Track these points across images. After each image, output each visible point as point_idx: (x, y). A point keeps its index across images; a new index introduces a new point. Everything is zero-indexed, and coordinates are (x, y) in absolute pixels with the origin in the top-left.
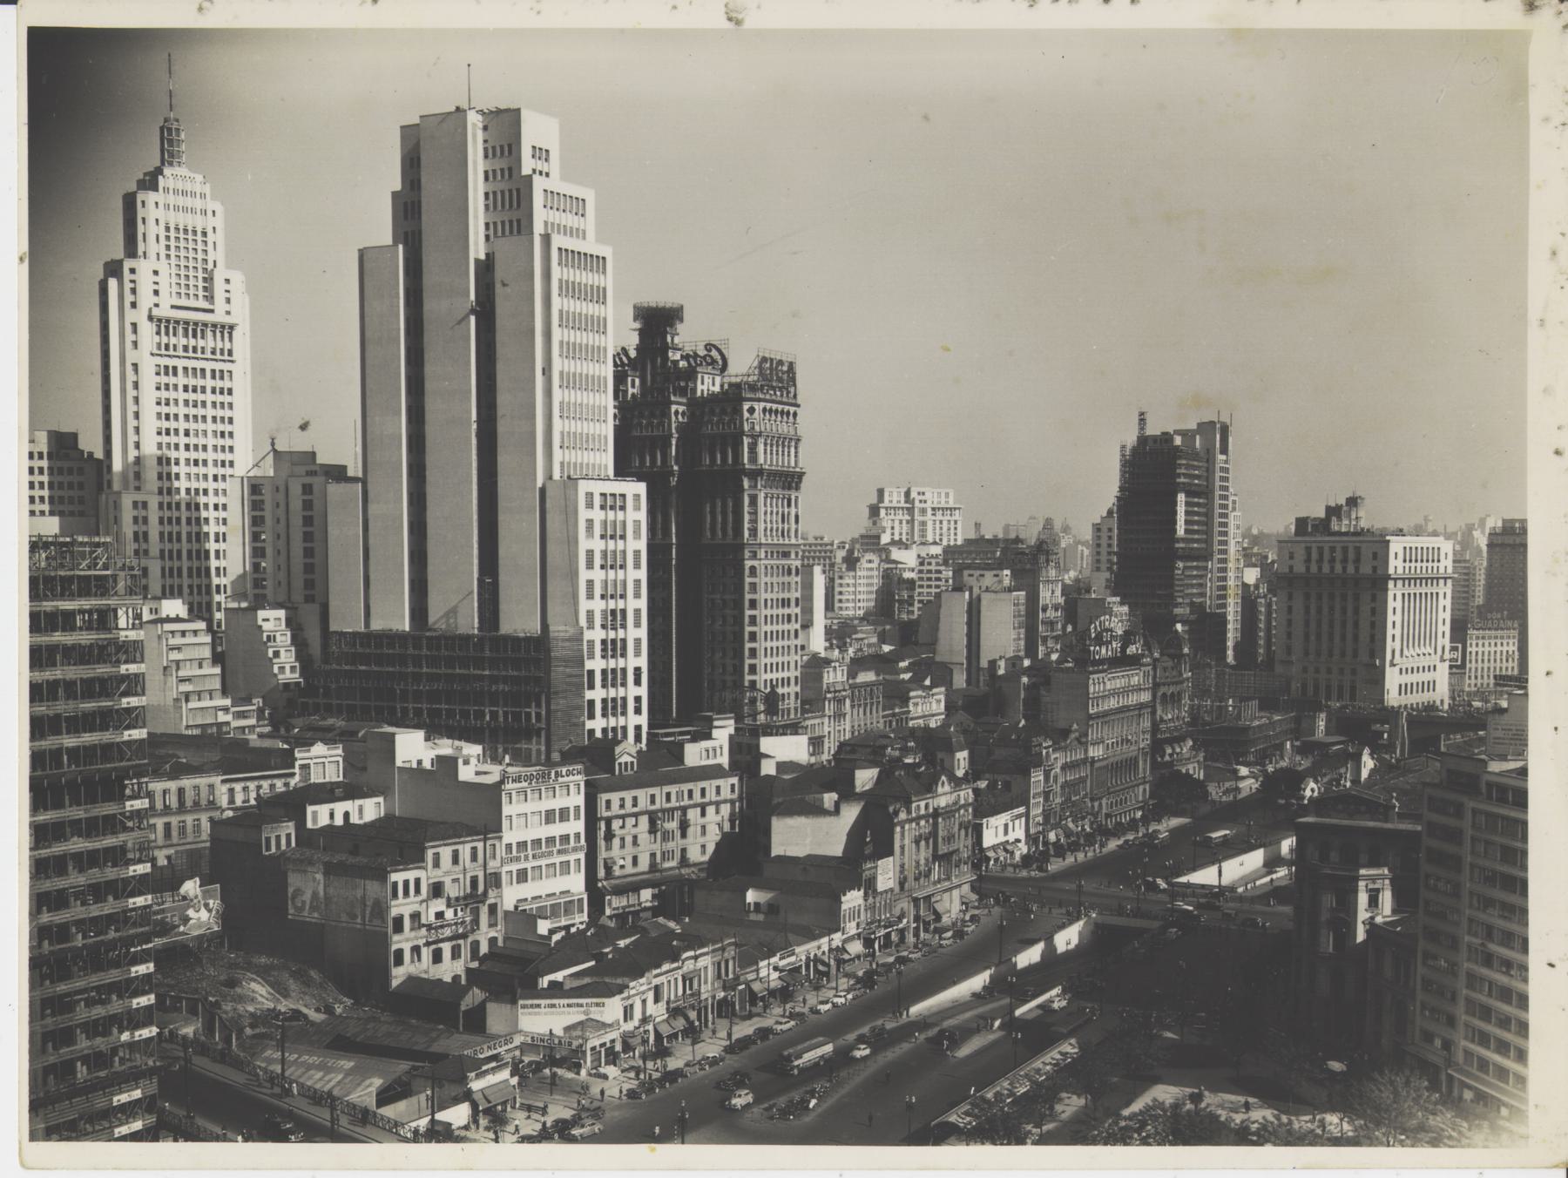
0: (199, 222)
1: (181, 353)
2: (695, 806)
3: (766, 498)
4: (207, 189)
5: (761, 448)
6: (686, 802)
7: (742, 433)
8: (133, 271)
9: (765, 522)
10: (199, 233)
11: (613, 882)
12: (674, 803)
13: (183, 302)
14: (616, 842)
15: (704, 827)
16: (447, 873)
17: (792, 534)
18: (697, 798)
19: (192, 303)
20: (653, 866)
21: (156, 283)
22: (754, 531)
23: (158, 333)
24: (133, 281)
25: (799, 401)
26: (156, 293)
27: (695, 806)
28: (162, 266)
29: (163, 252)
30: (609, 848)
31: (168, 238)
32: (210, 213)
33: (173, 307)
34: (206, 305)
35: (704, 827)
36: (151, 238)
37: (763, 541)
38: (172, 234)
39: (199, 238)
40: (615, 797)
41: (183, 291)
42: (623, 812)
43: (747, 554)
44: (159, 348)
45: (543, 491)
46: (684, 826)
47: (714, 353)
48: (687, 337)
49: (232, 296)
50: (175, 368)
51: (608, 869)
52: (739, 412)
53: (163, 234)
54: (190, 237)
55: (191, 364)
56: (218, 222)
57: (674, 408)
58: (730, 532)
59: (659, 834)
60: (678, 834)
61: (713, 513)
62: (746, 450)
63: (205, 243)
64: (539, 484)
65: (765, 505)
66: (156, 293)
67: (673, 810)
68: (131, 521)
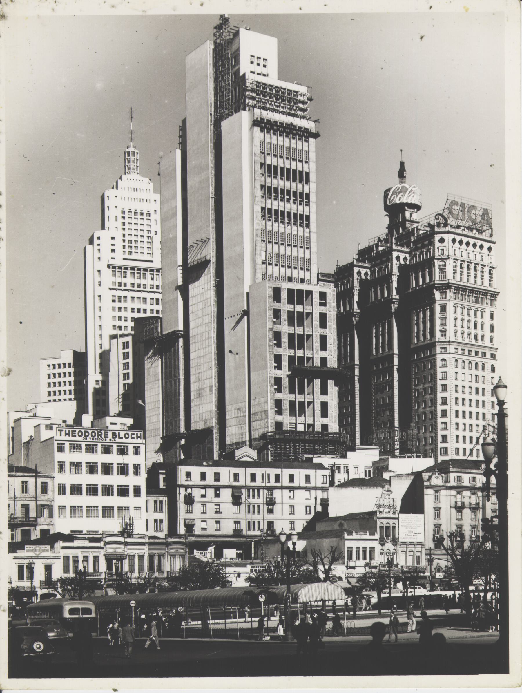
0: (145, 207)
2: (282, 488)
4: (151, 186)
5: (449, 269)
6: (273, 483)
7: (433, 258)
8: (99, 238)
10: (145, 214)
11: (193, 539)
12: (258, 482)
14: (197, 508)
15: (292, 507)
17: (487, 339)
18: (285, 481)
20: (237, 533)
22: (444, 332)
24: (99, 245)
26: (113, 251)
27: (282, 488)
29: (120, 227)
30: (189, 512)
33: (124, 259)
34: (149, 258)
35: (292, 507)
36: (112, 219)
37: (453, 339)
39: (145, 217)
40: (196, 471)
42: (203, 483)
43: (438, 350)
45: (248, 294)
46: (271, 502)
51: (189, 528)
52: (432, 243)
53: (120, 215)
54: (139, 216)
56: (158, 206)
57: (395, 254)
58: (428, 336)
59: (243, 506)
60: (264, 509)
61: (418, 324)
64: (247, 290)
65: (455, 312)
66: (113, 251)
67: (259, 488)
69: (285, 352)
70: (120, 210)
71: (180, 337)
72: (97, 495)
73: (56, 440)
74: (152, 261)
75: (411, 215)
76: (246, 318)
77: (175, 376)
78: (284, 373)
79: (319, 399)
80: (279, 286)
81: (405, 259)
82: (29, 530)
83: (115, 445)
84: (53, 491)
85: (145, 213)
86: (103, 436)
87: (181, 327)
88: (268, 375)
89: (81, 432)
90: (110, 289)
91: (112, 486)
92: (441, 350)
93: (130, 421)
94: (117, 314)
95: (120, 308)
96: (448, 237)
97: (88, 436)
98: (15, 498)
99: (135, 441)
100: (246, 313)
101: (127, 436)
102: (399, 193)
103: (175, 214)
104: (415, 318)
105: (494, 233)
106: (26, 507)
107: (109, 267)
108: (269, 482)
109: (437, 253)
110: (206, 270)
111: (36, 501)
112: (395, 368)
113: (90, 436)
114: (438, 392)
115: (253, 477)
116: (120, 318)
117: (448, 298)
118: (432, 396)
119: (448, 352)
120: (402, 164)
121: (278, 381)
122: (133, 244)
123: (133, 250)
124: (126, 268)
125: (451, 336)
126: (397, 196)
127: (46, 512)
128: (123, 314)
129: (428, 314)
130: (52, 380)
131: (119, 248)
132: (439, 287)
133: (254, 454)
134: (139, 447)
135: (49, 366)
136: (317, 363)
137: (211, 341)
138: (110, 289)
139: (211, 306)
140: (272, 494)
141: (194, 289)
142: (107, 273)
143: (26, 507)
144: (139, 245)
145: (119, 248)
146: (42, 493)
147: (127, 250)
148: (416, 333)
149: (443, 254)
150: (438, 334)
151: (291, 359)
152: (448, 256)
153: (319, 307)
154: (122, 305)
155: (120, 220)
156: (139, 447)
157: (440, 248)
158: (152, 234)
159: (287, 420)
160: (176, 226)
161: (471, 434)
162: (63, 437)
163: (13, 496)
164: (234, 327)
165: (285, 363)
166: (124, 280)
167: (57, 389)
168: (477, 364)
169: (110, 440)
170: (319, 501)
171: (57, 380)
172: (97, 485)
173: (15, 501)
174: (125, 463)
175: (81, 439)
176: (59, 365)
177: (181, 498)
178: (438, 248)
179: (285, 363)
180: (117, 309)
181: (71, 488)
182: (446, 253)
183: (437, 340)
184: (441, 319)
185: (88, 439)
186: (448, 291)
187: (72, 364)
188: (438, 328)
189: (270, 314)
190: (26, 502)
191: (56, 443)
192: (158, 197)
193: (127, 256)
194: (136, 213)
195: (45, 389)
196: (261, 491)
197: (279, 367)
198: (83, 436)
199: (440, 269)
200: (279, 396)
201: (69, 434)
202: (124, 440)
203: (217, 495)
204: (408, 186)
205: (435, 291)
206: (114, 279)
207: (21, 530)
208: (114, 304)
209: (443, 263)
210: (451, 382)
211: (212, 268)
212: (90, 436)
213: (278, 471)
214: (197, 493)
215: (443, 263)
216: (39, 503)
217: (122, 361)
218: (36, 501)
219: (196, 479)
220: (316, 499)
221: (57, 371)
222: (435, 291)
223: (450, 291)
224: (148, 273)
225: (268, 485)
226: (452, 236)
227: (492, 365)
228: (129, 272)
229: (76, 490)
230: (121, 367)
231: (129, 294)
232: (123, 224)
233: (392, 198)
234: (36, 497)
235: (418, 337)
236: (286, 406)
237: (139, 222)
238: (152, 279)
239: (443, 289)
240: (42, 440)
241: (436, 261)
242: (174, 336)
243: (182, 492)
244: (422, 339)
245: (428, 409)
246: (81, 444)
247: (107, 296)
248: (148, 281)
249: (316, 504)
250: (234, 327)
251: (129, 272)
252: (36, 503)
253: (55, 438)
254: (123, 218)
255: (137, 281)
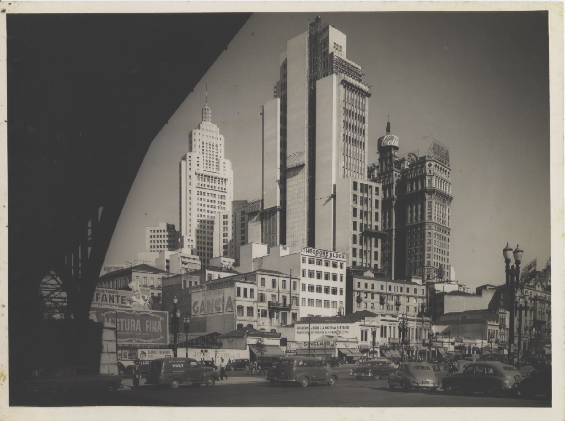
0: (215, 142)
2: (404, 296)
3: (436, 203)
6: (399, 292)
9: (435, 214)
10: (215, 146)
12: (392, 292)
13: (208, 169)
15: (408, 307)
16: (268, 291)
21: (198, 162)
22: (430, 217)
24: (190, 161)
26: (198, 165)
29: (201, 152)
35: (408, 307)
37: (434, 221)
39: (215, 147)
42: (366, 290)
43: (427, 227)
46: (398, 304)
53: (201, 145)
54: (211, 147)
55: (208, 191)
58: (419, 219)
59: (385, 305)
60: (395, 307)
61: (411, 213)
62: (427, 182)
64: (334, 182)
66: (198, 165)
69: (358, 220)
71: (278, 211)
72: (321, 292)
73: (302, 255)
74: (219, 173)
75: (394, 152)
76: (332, 199)
77: (273, 233)
78: (358, 232)
79: (374, 249)
80: (356, 181)
81: (399, 176)
82: (286, 313)
83: (331, 261)
84: (299, 288)
85: (215, 145)
86: (325, 254)
87: (278, 204)
88: (350, 233)
89: (314, 251)
90: (196, 187)
91: (329, 287)
92: (428, 227)
93: (233, 261)
94: (200, 202)
95: (201, 199)
96: (433, 164)
97: (318, 254)
98: (279, 291)
99: (341, 259)
100: (334, 196)
101: (337, 256)
102: (390, 139)
103: (277, 137)
104: (409, 209)
105: (450, 164)
106: (284, 298)
107: (196, 174)
108: (397, 291)
109: (427, 172)
110: (301, 171)
111: (290, 294)
112: (394, 237)
113: (319, 254)
114: (426, 251)
115: (390, 287)
116: (201, 205)
117: (433, 198)
118: (421, 253)
119: (432, 228)
120: (389, 124)
121: (355, 237)
122: (208, 163)
123: (208, 166)
124: (205, 176)
125: (433, 220)
126: (388, 141)
127: (295, 301)
128: (203, 202)
129: (420, 206)
130: (153, 239)
131: (201, 163)
132: (429, 191)
133: (372, 275)
134: (343, 263)
135: (151, 231)
136: (373, 228)
137: (304, 213)
138: (196, 187)
139: (304, 192)
140: (398, 299)
141: (291, 182)
142: (195, 177)
143: (284, 298)
144: (211, 163)
146: (293, 289)
147: (205, 166)
148: (415, 216)
150: (427, 218)
151: (361, 225)
152: (434, 174)
153: (375, 196)
154: (203, 197)
155: (201, 148)
156: (343, 263)
157: (429, 169)
158: (218, 158)
159: (358, 260)
160: (277, 144)
162: (305, 253)
163: (278, 290)
164: (324, 204)
165: (358, 227)
166: (204, 183)
167: (156, 244)
169: (329, 257)
170: (420, 304)
171: (156, 239)
172: (321, 286)
173: (279, 293)
174: (336, 273)
175: (314, 255)
176: (158, 231)
177: (355, 298)
178: (428, 169)
179: (358, 227)
180: (200, 199)
181: (308, 287)
182: (432, 172)
183: (426, 221)
184: (428, 210)
185: (318, 256)
186: (433, 194)
187: (166, 230)
188: (427, 215)
189: (351, 197)
190: (285, 294)
191: (301, 257)
192: (222, 136)
194: (210, 144)
195: (148, 244)
196: (394, 296)
197: (355, 228)
198: (315, 254)
199: (429, 181)
200: (355, 246)
201: (308, 251)
202: (335, 258)
203: (373, 298)
204: (394, 136)
205: (426, 193)
206: (198, 182)
207: (282, 313)
208: (198, 196)
209: (430, 178)
210: (433, 246)
211: (306, 169)
212: (319, 254)
213: (402, 285)
214: (363, 295)
215: (430, 178)
216: (292, 295)
217: (222, 226)
218: (290, 294)
219: (362, 287)
220: (419, 304)
221: (156, 234)
222: (426, 193)
223: (434, 194)
224: (217, 180)
225: (397, 293)
226: (435, 163)
227: (448, 238)
228: (206, 178)
229: (311, 288)
230: (222, 229)
231: (207, 191)
232: (203, 150)
233: (385, 142)
234: (290, 292)
236: (358, 252)
237: (212, 150)
238: (219, 184)
239: (430, 193)
240: (281, 256)
241: (427, 177)
242: (273, 210)
243: (356, 295)
244: (414, 221)
245: (418, 261)
246: (314, 259)
247: (195, 191)
248: (217, 185)
249: (419, 306)
250: (324, 204)
251: (206, 178)
252: (290, 295)
253: (301, 253)
254: (203, 146)
255: (211, 184)
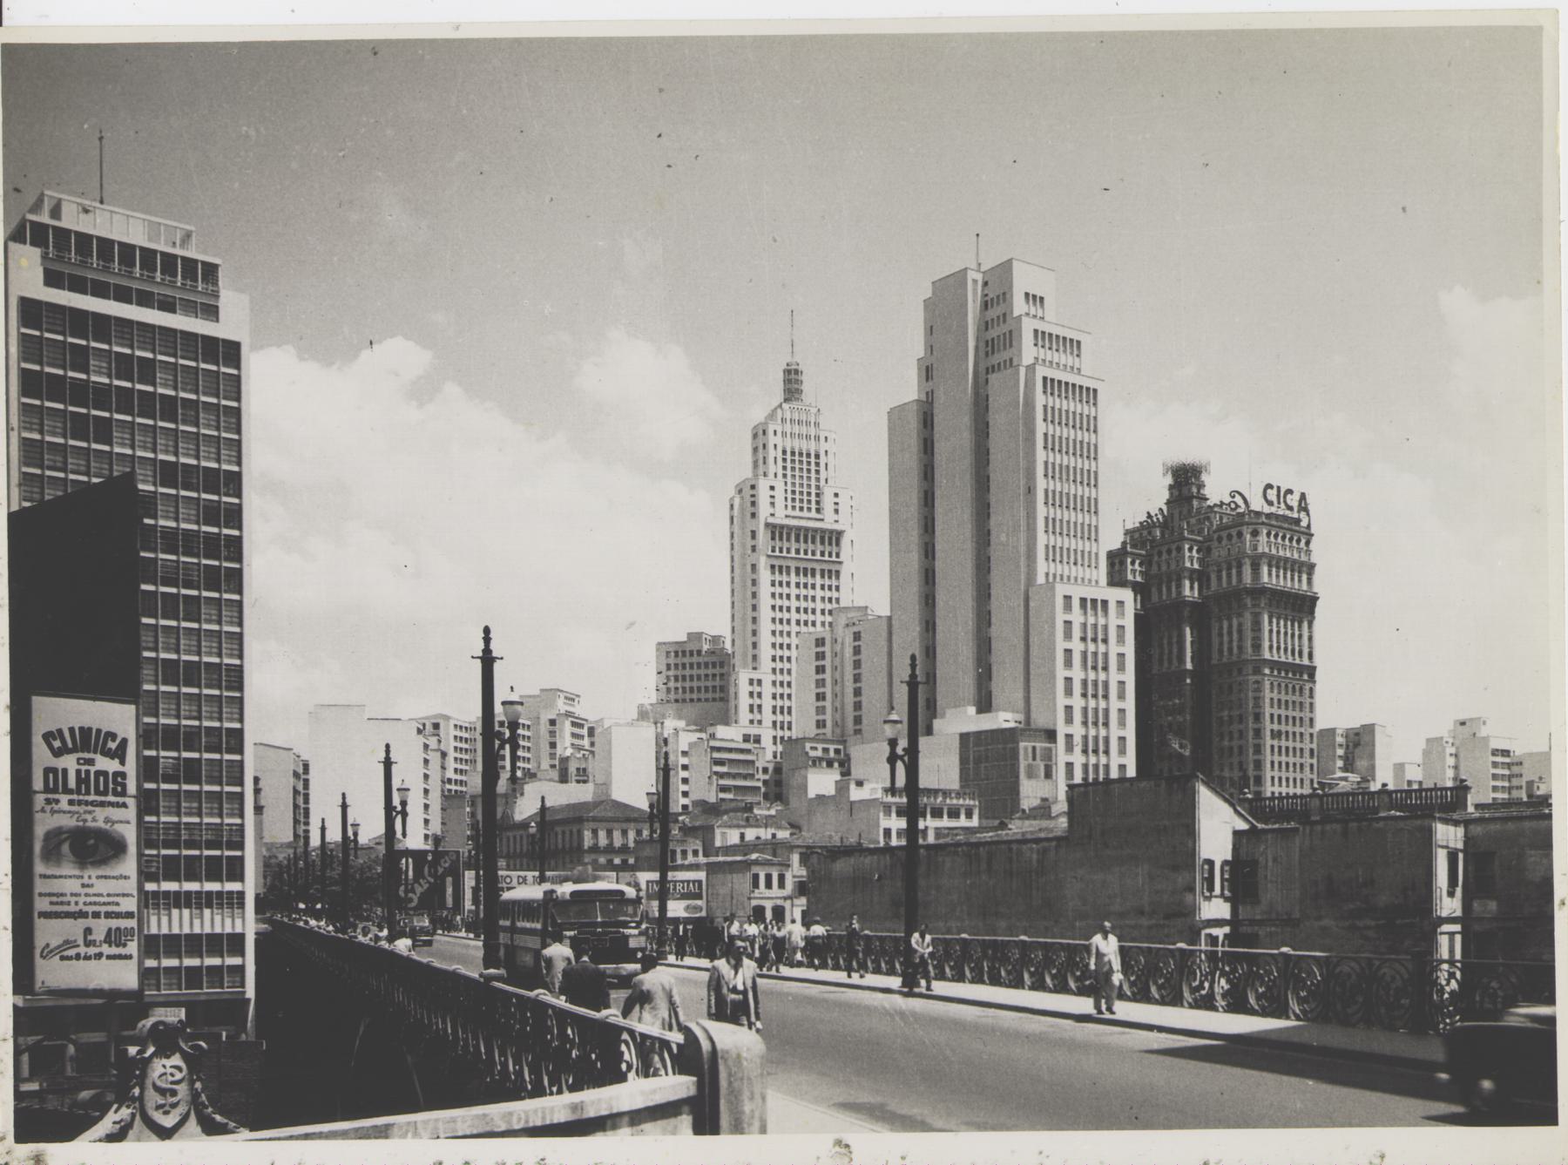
1: (793, 554)
13: (797, 513)
19: (805, 514)
23: (773, 539)
25: (1313, 531)
26: (773, 504)
28: (779, 485)
29: (780, 472)
31: (784, 460)
32: (822, 439)
37: (1267, 656)
38: (789, 457)
39: (813, 460)
41: (797, 504)
44: (773, 551)
47: (1238, 499)
48: (1215, 490)
49: (840, 508)
50: (788, 568)
58: (1235, 650)
61: (1221, 635)
63: (817, 464)
66: (773, 504)
68: (748, 709)
70: (780, 450)
99: (967, 802)
117: (1262, 605)
131: (780, 501)
145: (780, 501)
147: (790, 503)
149: (1256, 549)
161: (1287, 774)
168: (1294, 687)
193: (790, 512)
202: (955, 801)
235: (1221, 651)
